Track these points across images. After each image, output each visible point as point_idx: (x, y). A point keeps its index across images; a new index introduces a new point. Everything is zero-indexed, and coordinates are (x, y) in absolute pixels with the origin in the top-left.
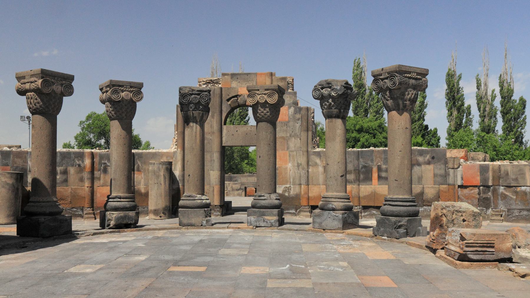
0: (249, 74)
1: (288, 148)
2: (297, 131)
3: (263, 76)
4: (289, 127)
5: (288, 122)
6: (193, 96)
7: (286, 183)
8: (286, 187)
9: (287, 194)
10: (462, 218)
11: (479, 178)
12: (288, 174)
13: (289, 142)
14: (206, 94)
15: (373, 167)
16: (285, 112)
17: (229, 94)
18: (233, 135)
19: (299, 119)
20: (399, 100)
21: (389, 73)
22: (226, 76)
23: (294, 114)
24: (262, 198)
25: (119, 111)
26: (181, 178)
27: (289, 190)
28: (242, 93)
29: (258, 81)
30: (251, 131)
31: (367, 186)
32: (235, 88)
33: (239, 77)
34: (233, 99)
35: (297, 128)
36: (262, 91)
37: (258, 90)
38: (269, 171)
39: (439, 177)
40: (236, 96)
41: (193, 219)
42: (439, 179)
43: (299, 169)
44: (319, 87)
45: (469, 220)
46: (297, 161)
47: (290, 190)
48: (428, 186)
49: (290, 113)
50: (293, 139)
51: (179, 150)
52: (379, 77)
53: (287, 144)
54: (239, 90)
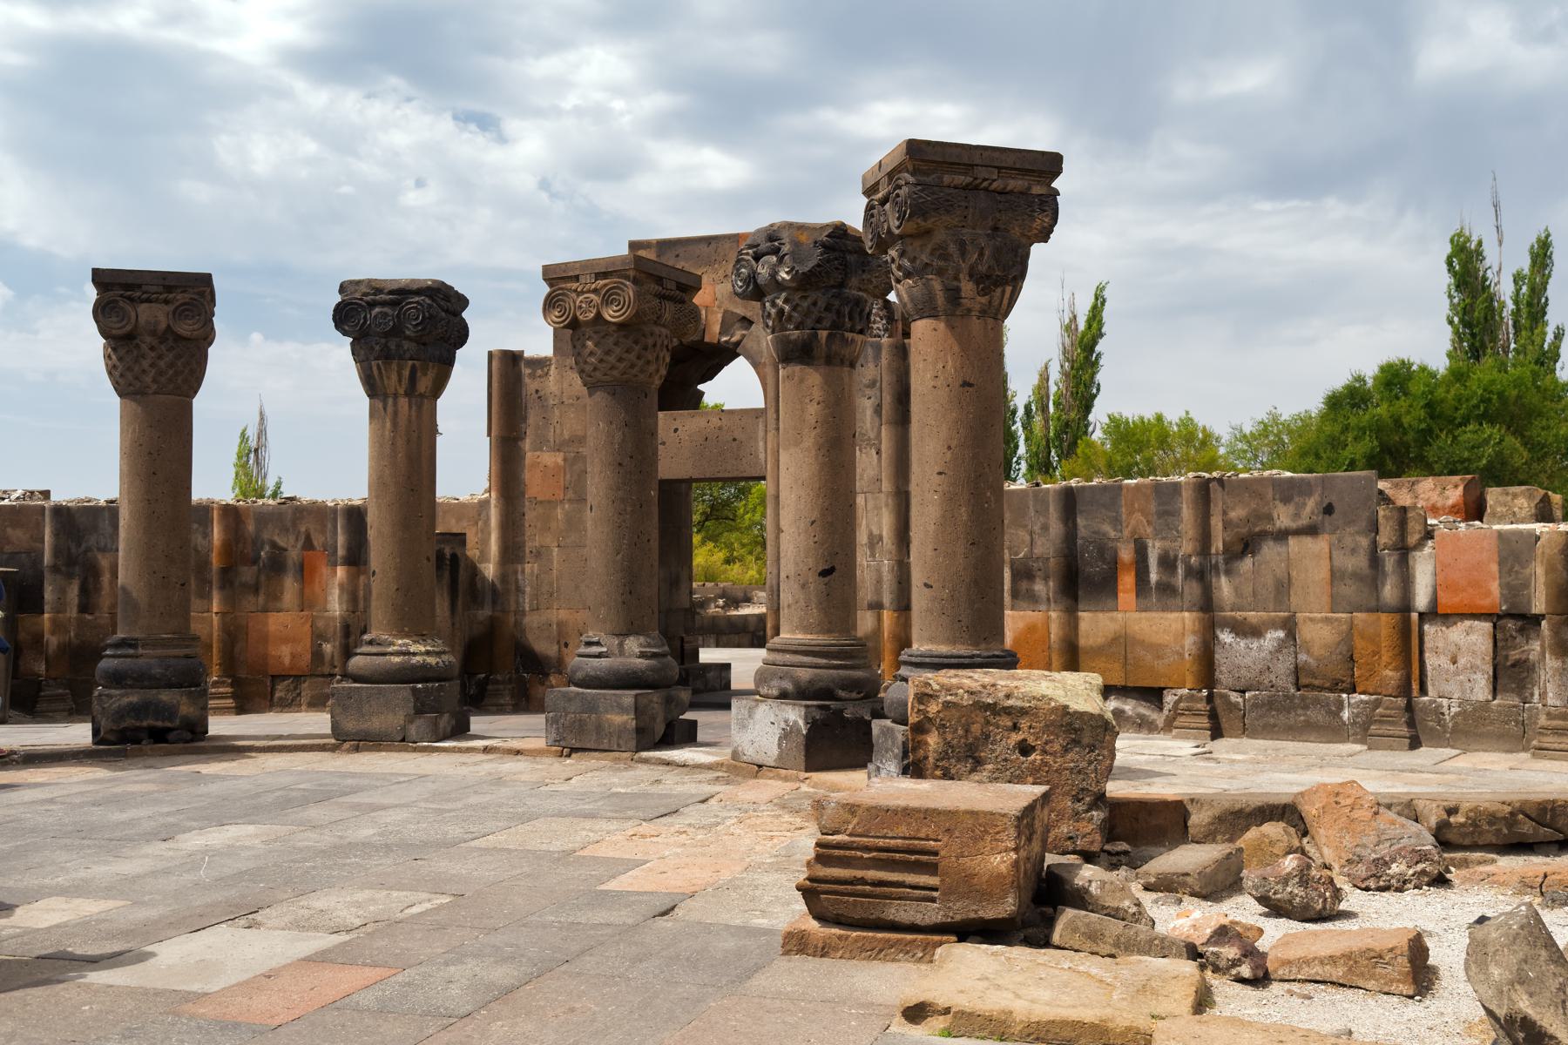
2: (868, 425)
6: (377, 310)
10: (1016, 737)
11: (1495, 588)
14: (417, 302)
20: (930, 277)
24: (595, 650)
25: (129, 369)
30: (720, 428)
31: (1100, 615)
36: (587, 281)
37: (576, 278)
38: (620, 557)
39: (1348, 582)
41: (374, 720)
42: (1348, 590)
43: (873, 555)
44: (747, 254)
45: (1047, 748)
46: (868, 526)
48: (1311, 615)
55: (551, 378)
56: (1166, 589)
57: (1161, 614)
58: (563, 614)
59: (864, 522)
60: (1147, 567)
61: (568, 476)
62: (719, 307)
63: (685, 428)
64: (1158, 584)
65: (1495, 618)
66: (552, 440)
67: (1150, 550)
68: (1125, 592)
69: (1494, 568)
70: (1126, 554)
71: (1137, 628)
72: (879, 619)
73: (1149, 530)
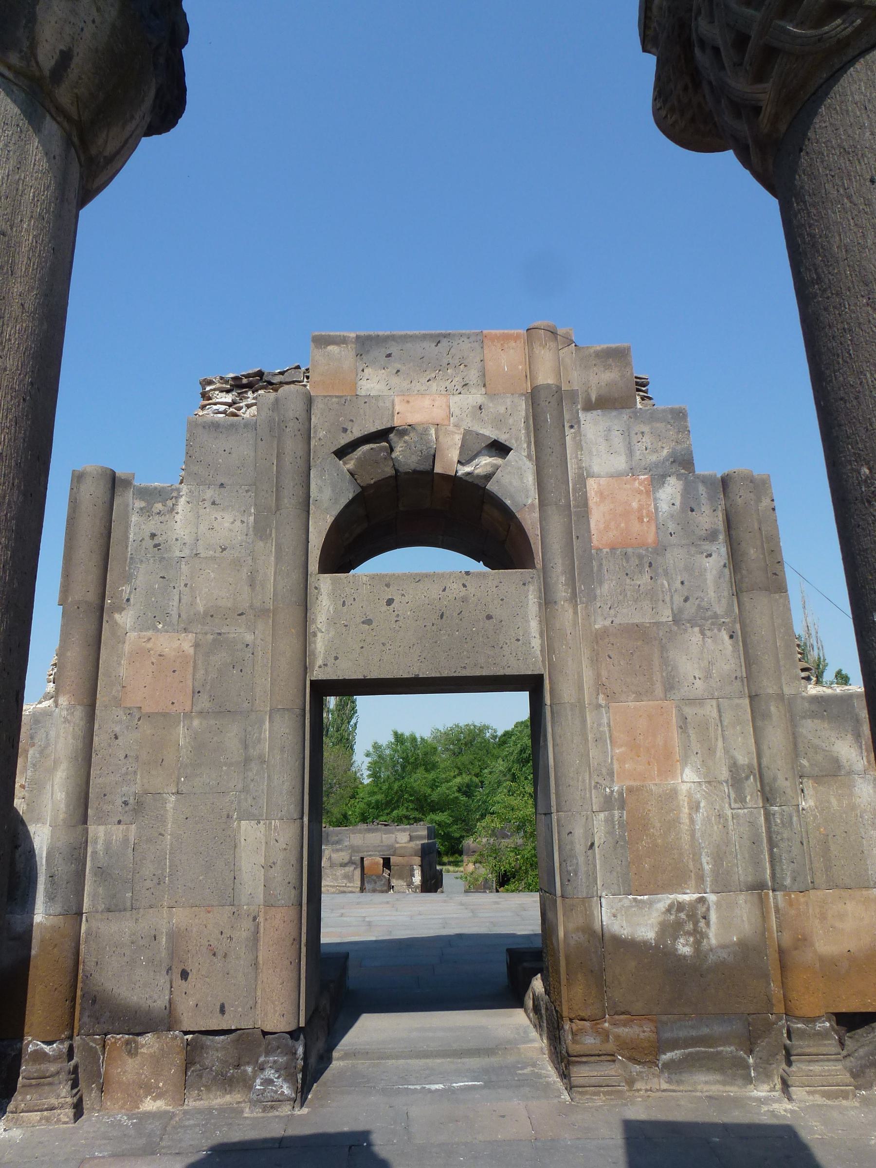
0: (445, 336)
1: (670, 686)
3: (512, 344)
7: (676, 883)
8: (680, 907)
9: (684, 948)
12: (685, 827)
16: (635, 505)
17: (348, 426)
18: (368, 622)
19: (712, 536)
22: (330, 348)
23: (683, 510)
26: (63, 869)
27: (696, 924)
28: (410, 422)
29: (490, 365)
30: (464, 600)
32: (377, 398)
33: (394, 349)
34: (367, 447)
35: (710, 577)
40: (382, 435)
46: (726, 751)
47: (702, 924)
49: (664, 507)
51: (63, 701)
54: (397, 408)
55: (178, 518)
58: (181, 917)
61: (200, 673)
62: (457, 426)
63: (406, 599)
66: (174, 613)
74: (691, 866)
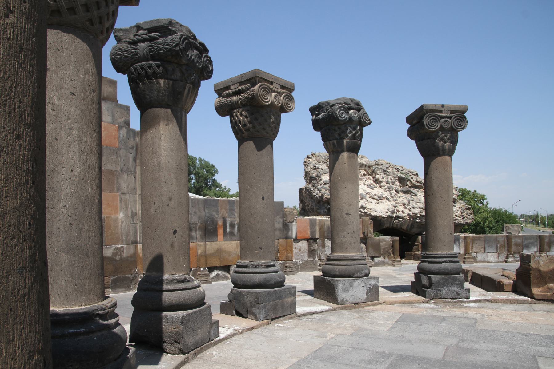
2: (131, 165)
4: (120, 156)
5: (119, 149)
7: (117, 243)
8: (117, 248)
11: (309, 232)
12: (119, 228)
13: (119, 180)
15: (218, 219)
21: (452, 112)
27: (121, 253)
31: (213, 243)
39: (278, 231)
43: (133, 221)
46: (131, 209)
47: (122, 253)
50: (126, 176)
52: (437, 114)
53: (118, 182)
56: (232, 234)
57: (230, 242)
59: (129, 206)
60: (226, 227)
64: (229, 232)
65: (308, 240)
67: (227, 221)
68: (220, 235)
69: (309, 227)
70: (220, 223)
71: (223, 246)
72: (136, 248)
73: (227, 215)
74: (121, 238)
